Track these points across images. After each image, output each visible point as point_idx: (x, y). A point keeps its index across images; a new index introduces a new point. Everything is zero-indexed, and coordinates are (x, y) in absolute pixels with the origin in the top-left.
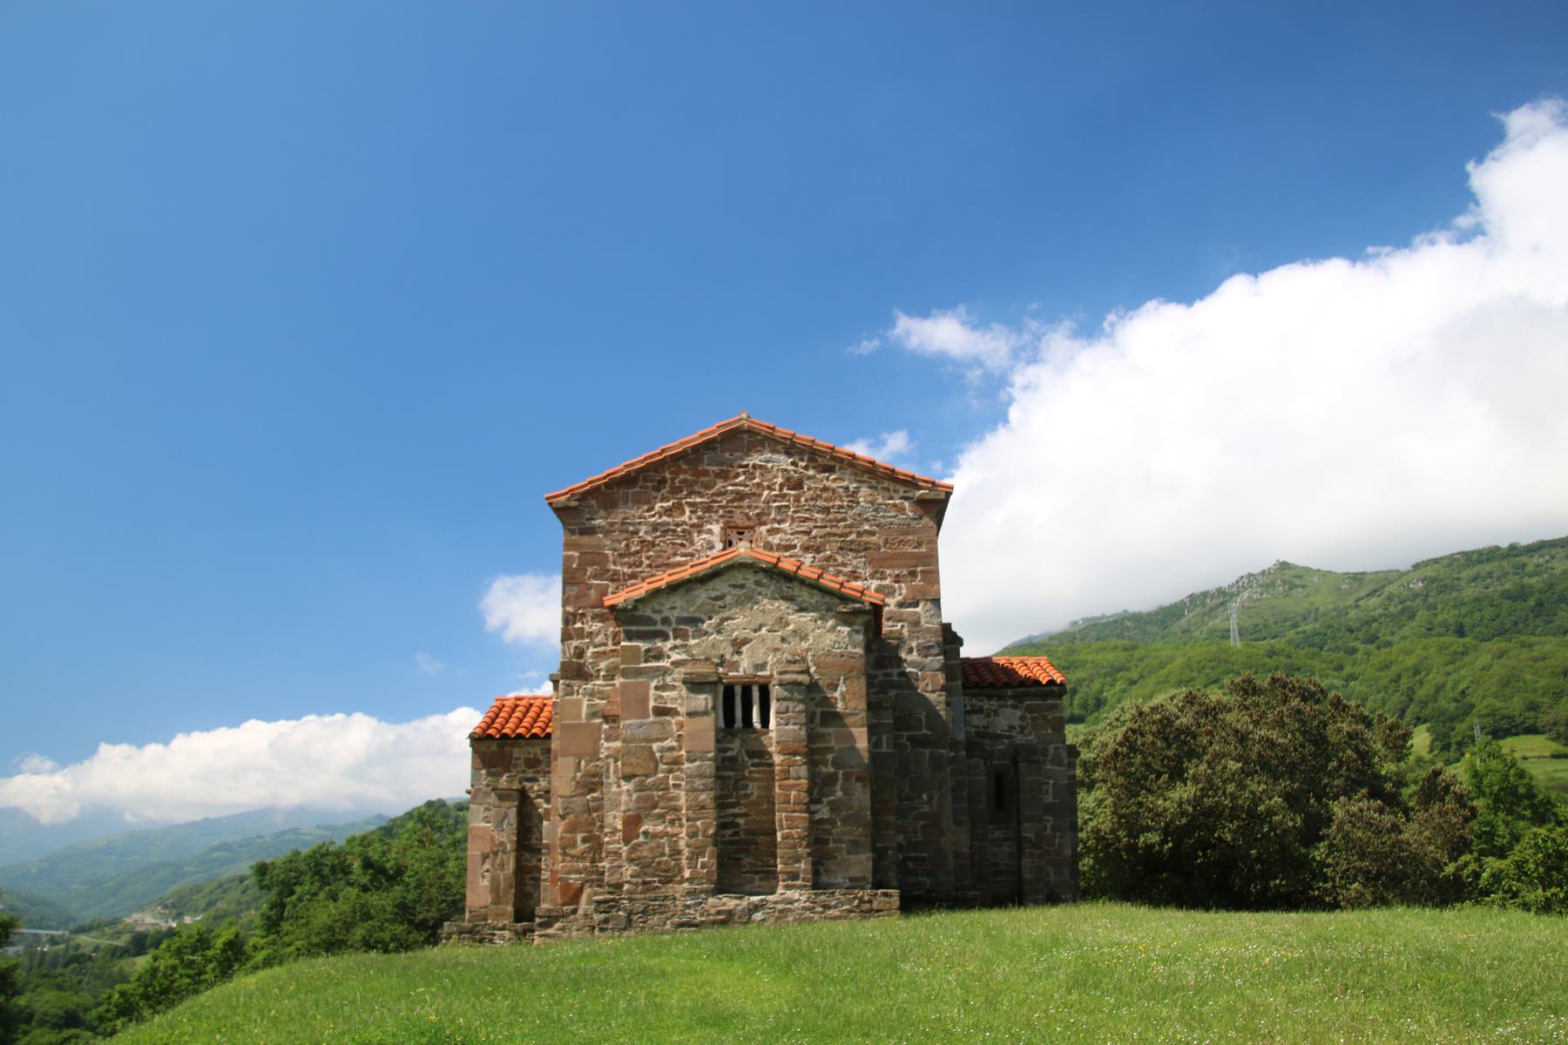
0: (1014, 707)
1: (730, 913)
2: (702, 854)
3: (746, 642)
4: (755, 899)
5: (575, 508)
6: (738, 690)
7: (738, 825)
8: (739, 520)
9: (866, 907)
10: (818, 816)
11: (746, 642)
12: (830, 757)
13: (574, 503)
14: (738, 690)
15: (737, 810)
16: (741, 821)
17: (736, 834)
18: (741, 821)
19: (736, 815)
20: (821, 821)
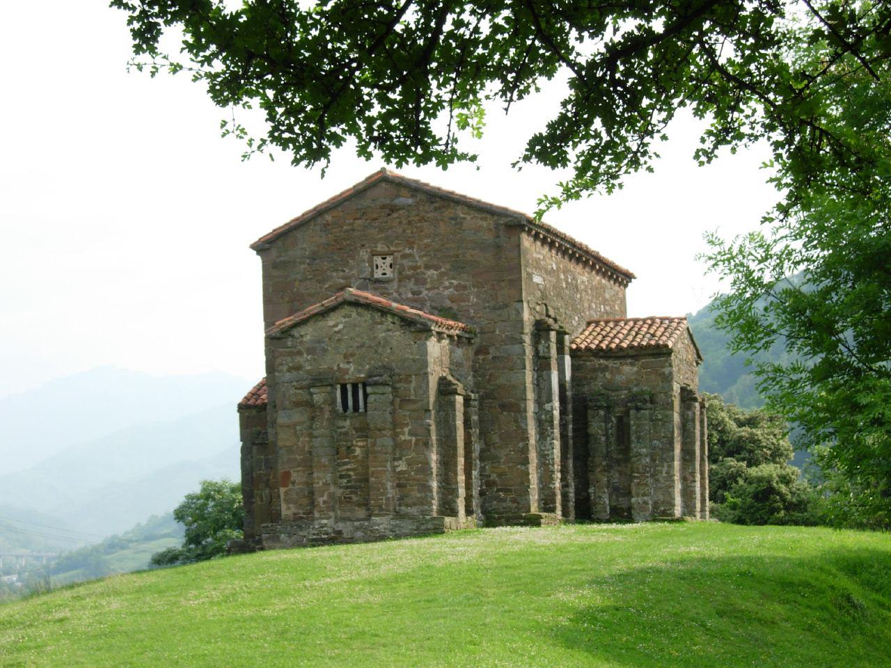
0: (632, 365)
1: (340, 533)
2: (323, 496)
3: (352, 355)
4: (357, 524)
5: (268, 249)
6: (349, 387)
7: (349, 476)
8: (380, 247)
9: (423, 527)
10: (399, 469)
11: (352, 355)
12: (406, 430)
13: (267, 246)
14: (349, 387)
15: (349, 467)
16: (352, 473)
17: (349, 482)
18: (352, 473)
19: (348, 470)
20: (401, 472)
